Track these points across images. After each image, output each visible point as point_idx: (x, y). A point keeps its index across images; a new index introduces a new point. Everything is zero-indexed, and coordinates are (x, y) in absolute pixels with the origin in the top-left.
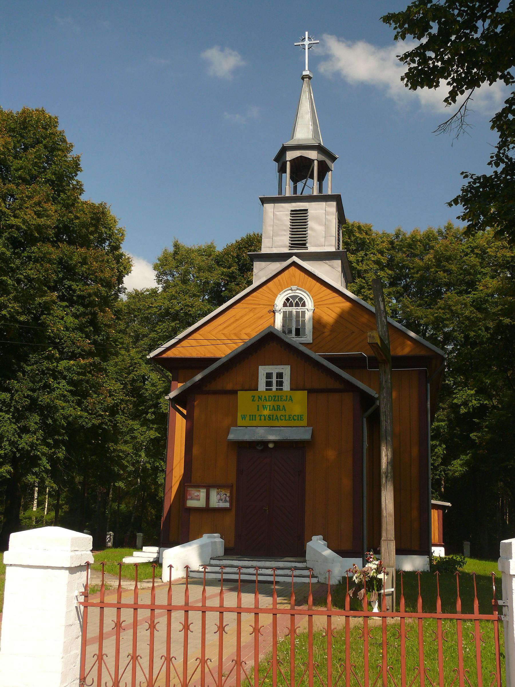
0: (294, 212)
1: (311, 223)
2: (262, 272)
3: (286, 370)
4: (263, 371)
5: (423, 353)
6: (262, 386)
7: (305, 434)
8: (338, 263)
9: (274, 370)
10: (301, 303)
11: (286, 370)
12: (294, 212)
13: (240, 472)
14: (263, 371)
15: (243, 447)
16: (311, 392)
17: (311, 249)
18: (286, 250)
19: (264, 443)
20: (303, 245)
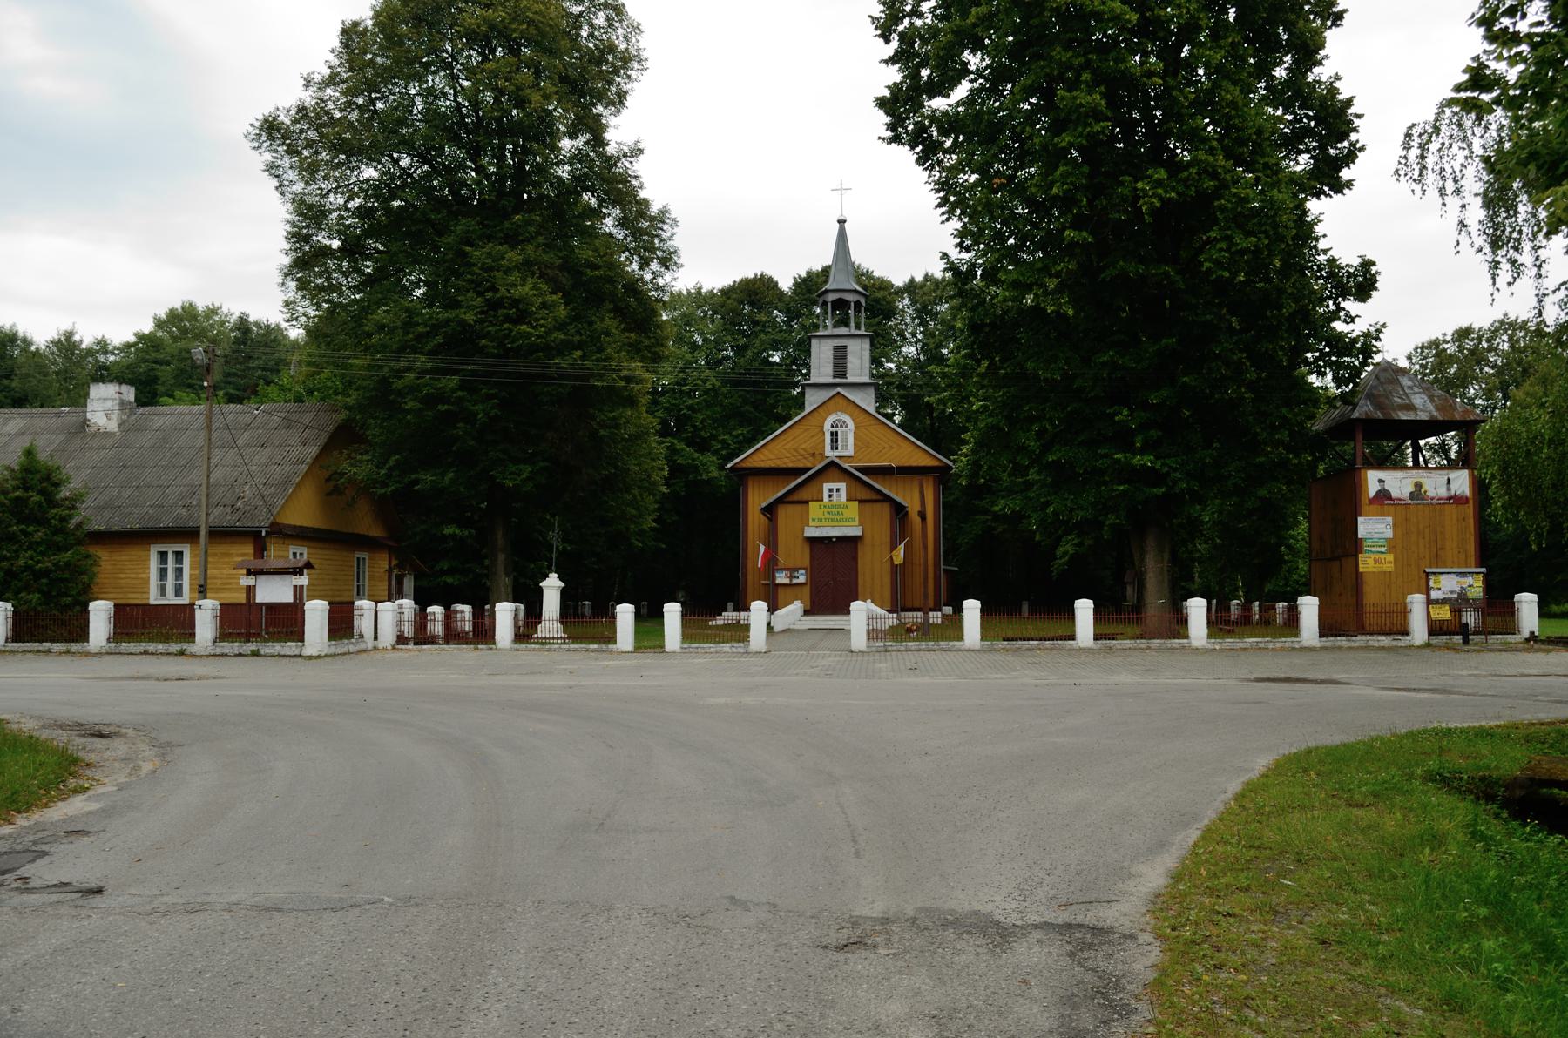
0: (836, 348)
1: (850, 358)
2: (813, 399)
3: (842, 486)
4: (826, 487)
5: (936, 463)
6: (826, 498)
7: (857, 532)
8: (871, 392)
9: (834, 486)
10: (844, 424)
11: (842, 486)
12: (836, 348)
13: (812, 558)
14: (826, 487)
15: (812, 541)
16: (861, 501)
17: (851, 379)
18: (831, 380)
19: (829, 538)
20: (844, 376)
